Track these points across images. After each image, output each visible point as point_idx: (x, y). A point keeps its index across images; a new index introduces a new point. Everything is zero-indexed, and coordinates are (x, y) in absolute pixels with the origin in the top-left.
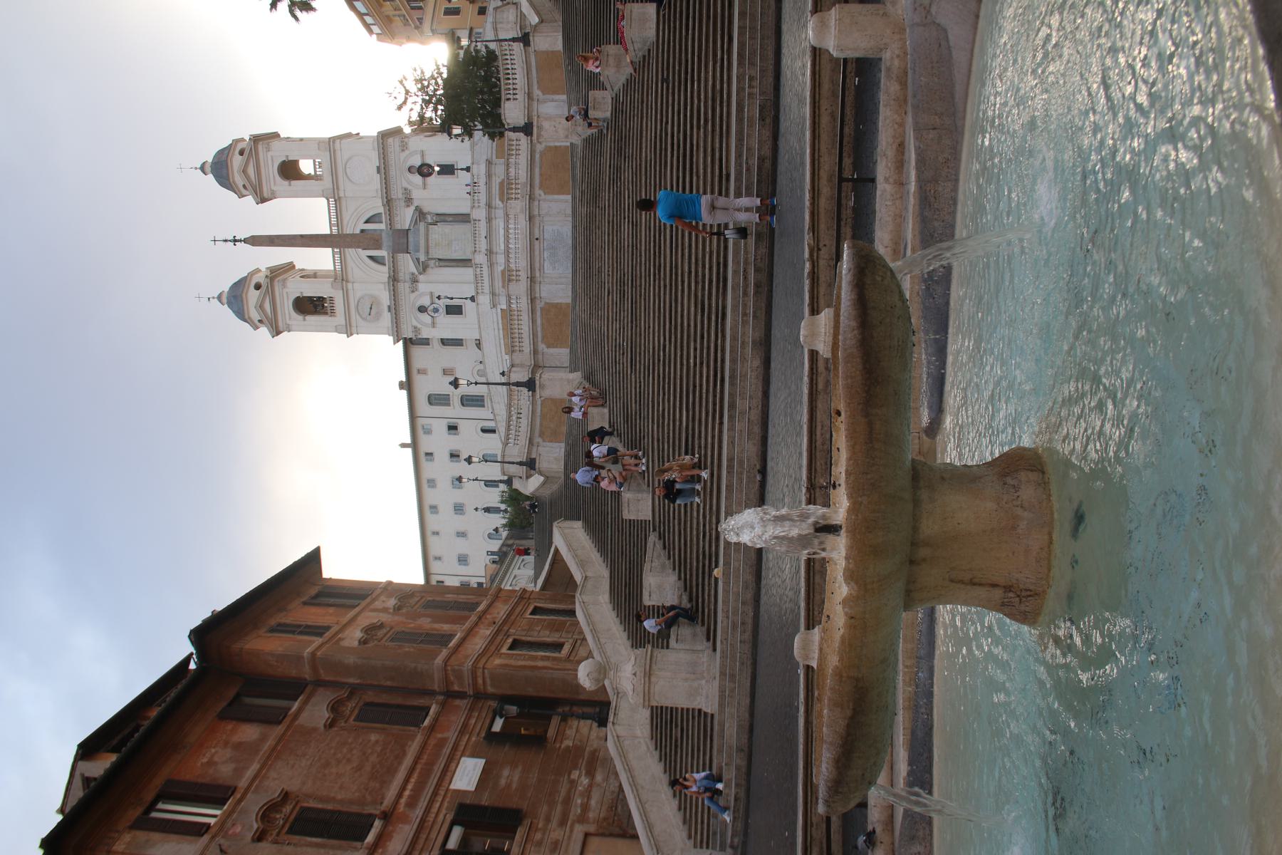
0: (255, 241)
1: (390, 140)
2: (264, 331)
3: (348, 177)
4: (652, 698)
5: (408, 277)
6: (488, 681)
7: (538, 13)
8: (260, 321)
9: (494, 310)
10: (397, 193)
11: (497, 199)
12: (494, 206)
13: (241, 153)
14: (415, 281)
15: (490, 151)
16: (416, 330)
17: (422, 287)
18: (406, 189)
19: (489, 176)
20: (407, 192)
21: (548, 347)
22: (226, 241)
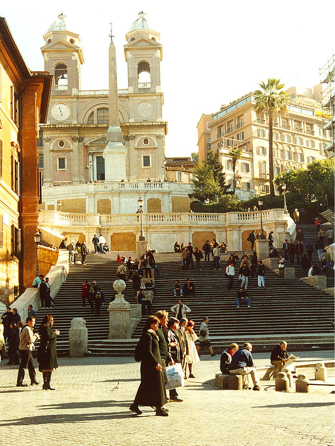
0: (112, 49)
1: (163, 129)
2: (43, 43)
3: (141, 102)
4: (113, 312)
5: (82, 136)
6: (30, 224)
7: (292, 234)
8: (50, 41)
9: (85, 194)
10: (132, 133)
11: (150, 197)
12: (146, 195)
13: (153, 39)
14: (80, 140)
15: (175, 193)
16: (49, 140)
17: (76, 144)
18: (134, 137)
19: (163, 193)
20: (134, 137)
21: (112, 237)
22: (111, 31)
